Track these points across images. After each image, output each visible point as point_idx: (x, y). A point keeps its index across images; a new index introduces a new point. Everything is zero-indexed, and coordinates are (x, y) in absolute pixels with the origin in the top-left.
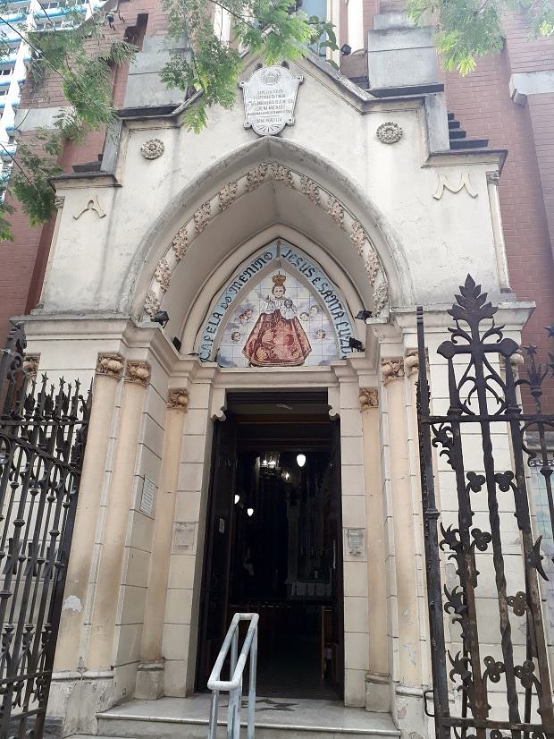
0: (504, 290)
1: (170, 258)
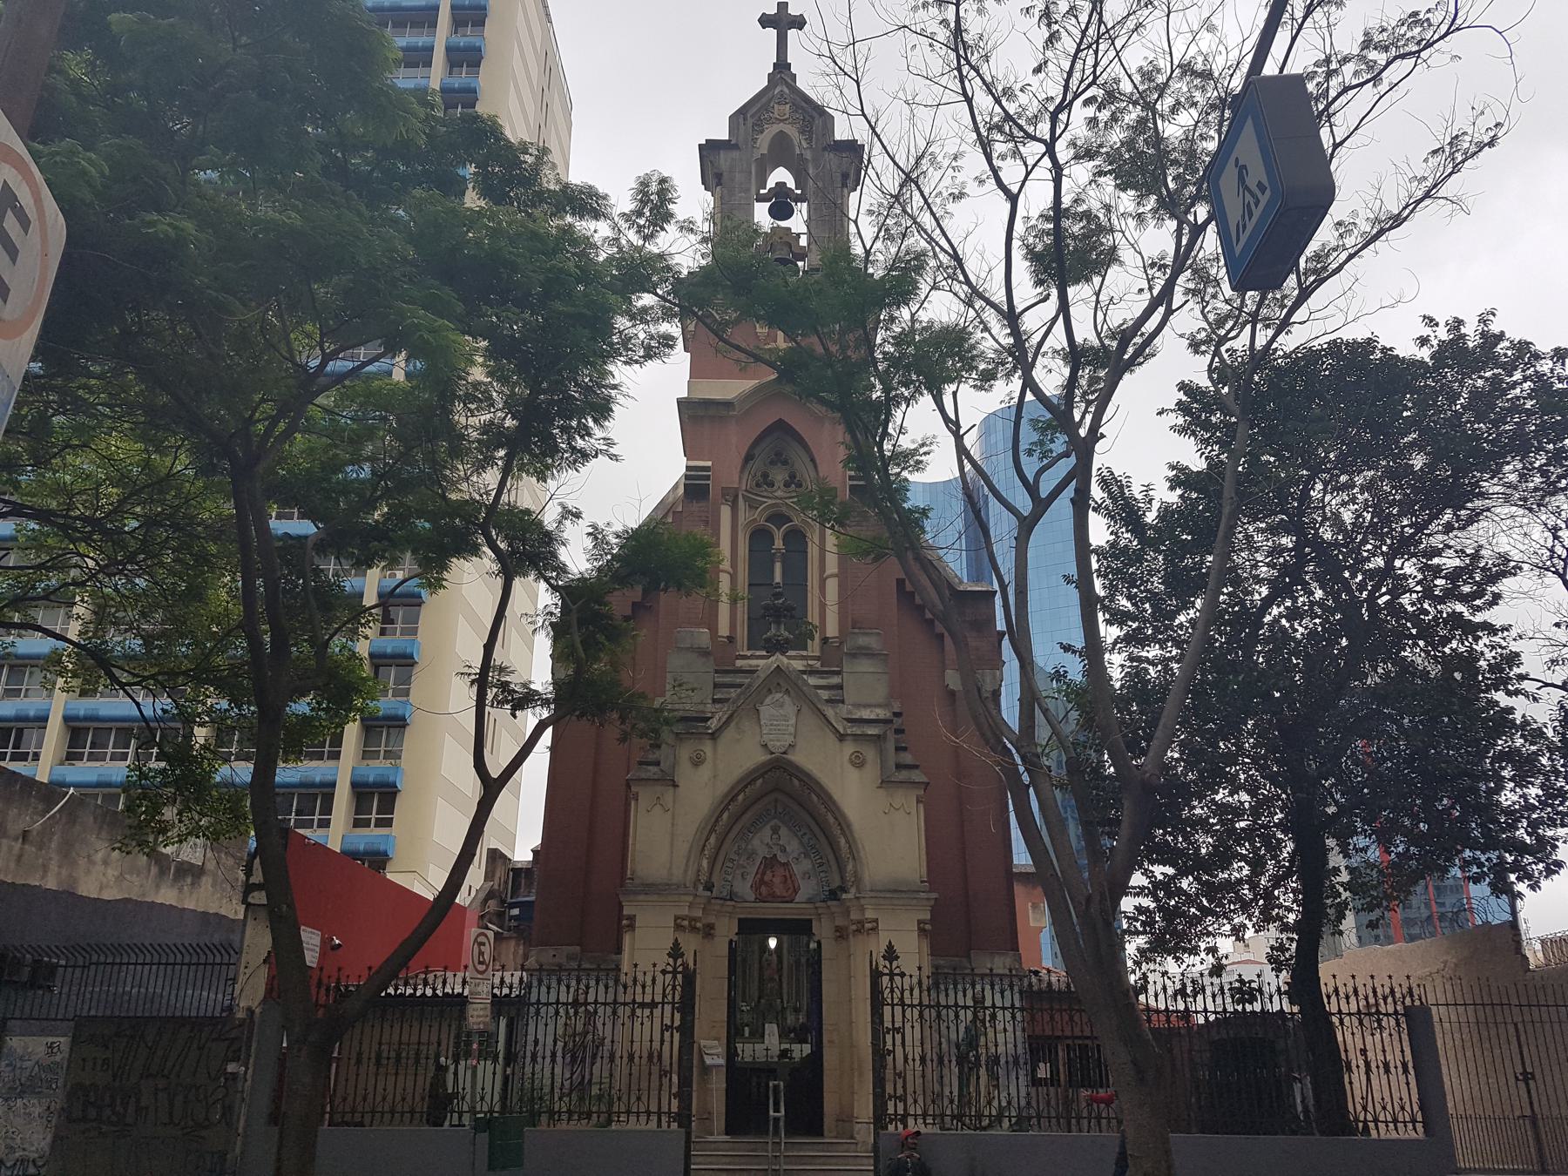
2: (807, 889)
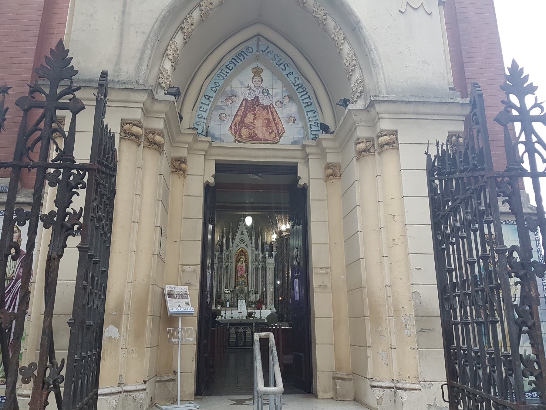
0: (451, 89)
1: (179, 39)
2: (292, 132)
